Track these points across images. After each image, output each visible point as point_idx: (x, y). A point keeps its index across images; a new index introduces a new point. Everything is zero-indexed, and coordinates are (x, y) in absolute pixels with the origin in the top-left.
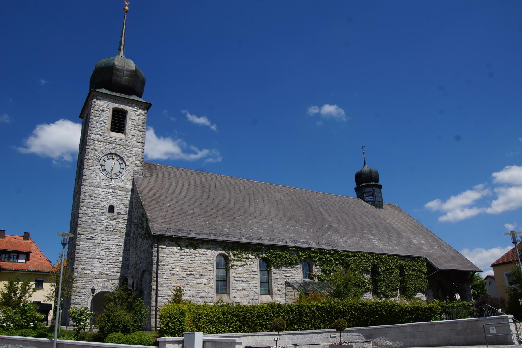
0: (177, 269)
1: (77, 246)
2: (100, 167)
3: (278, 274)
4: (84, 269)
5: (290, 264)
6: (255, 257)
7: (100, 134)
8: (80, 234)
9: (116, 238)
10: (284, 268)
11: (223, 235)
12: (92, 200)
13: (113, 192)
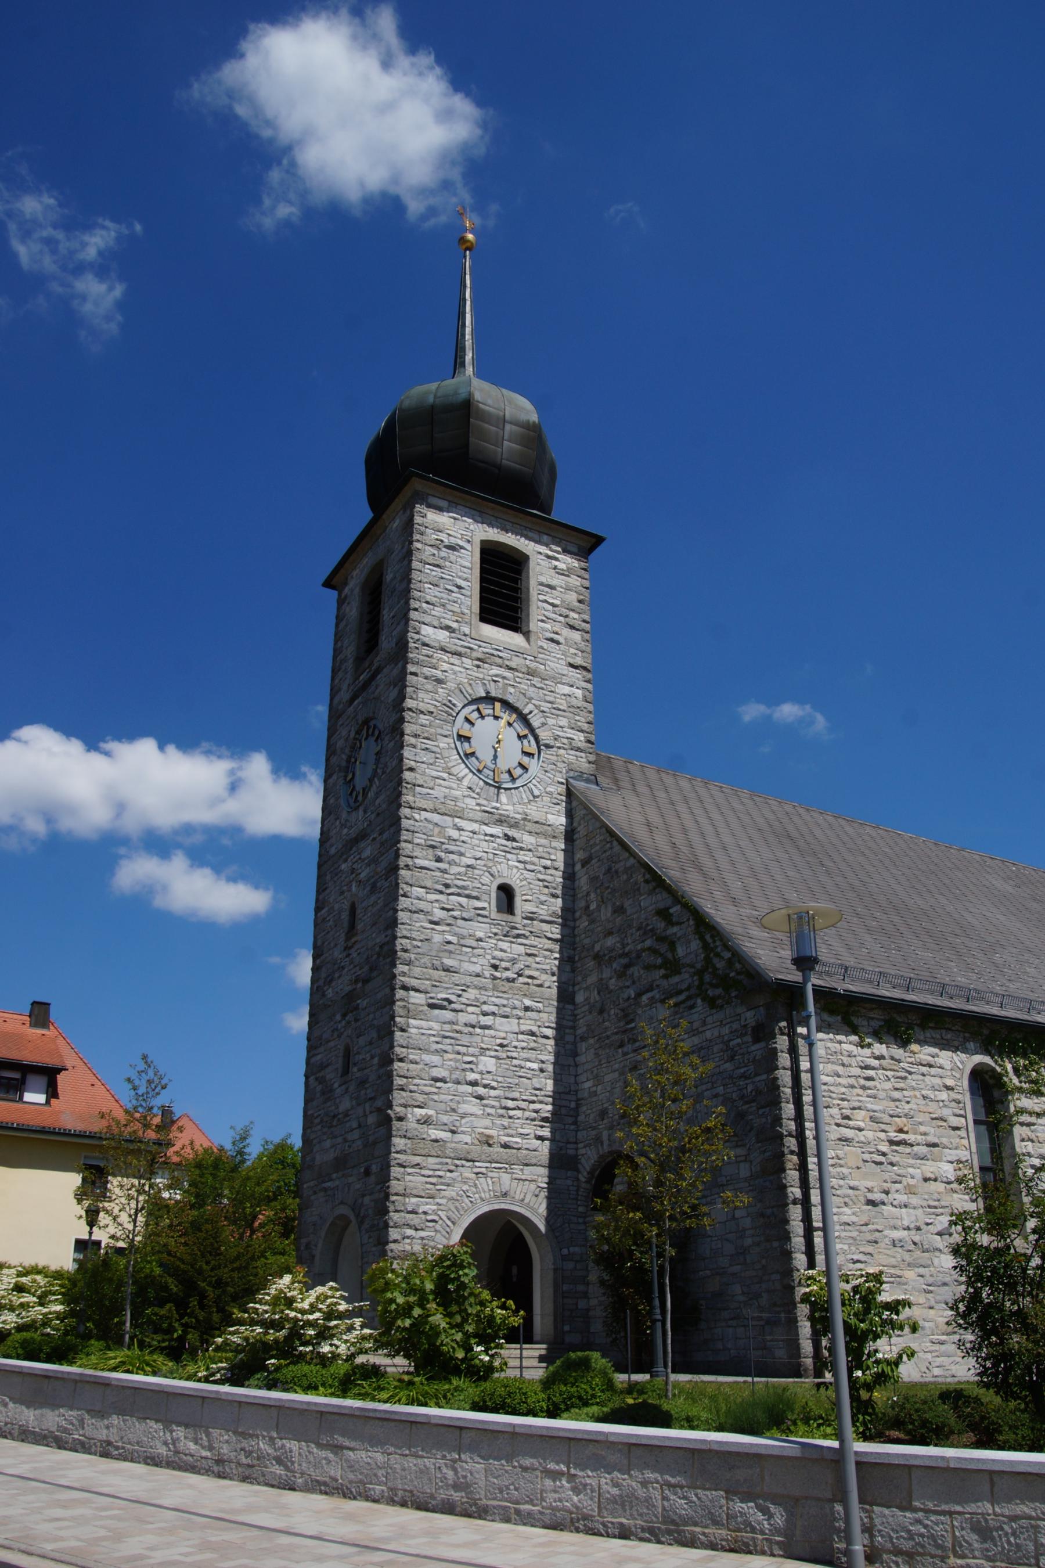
1: (398, 1034)
2: (458, 744)
7: (447, 628)
8: (405, 988)
9: (527, 1009)
12: (439, 860)
13: (508, 838)
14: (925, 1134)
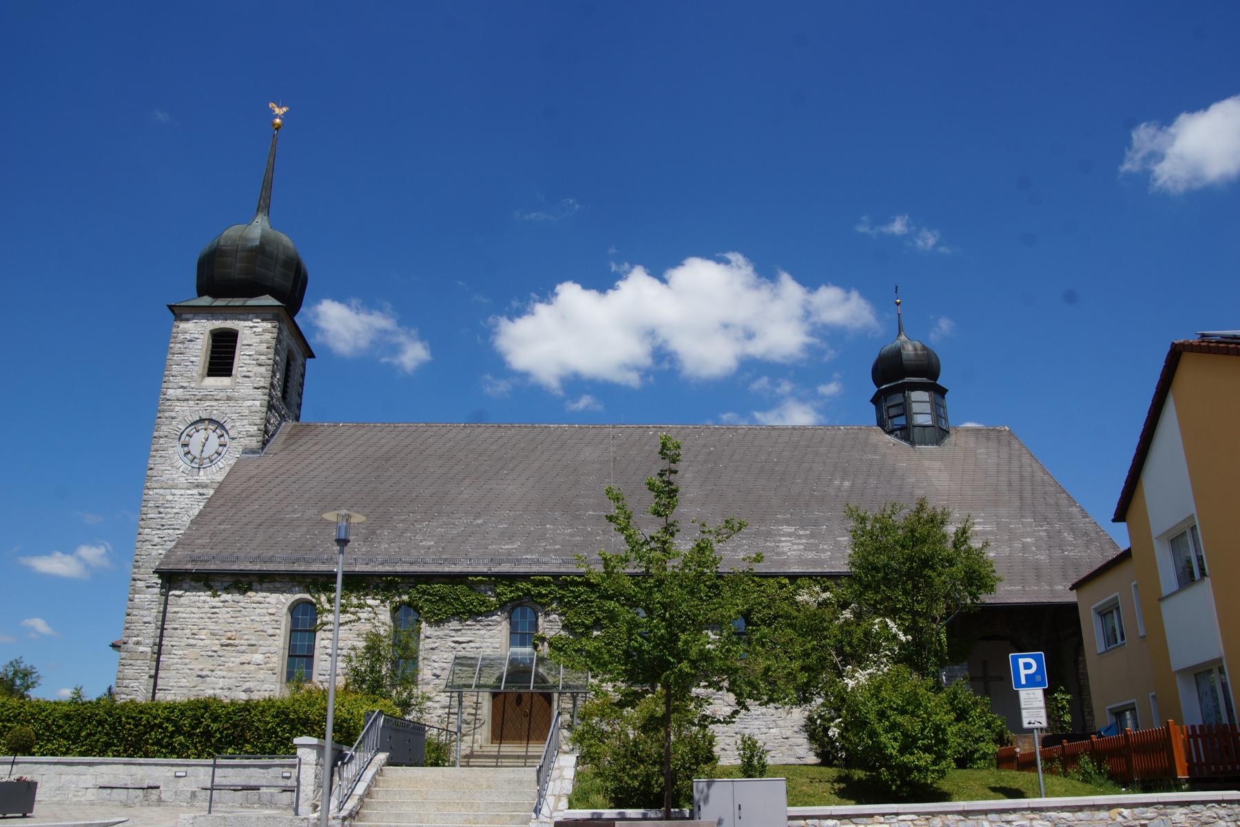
3: (438, 637)
4: (138, 643)
5: (472, 614)
7: (182, 387)
10: (454, 624)
11: (314, 561)
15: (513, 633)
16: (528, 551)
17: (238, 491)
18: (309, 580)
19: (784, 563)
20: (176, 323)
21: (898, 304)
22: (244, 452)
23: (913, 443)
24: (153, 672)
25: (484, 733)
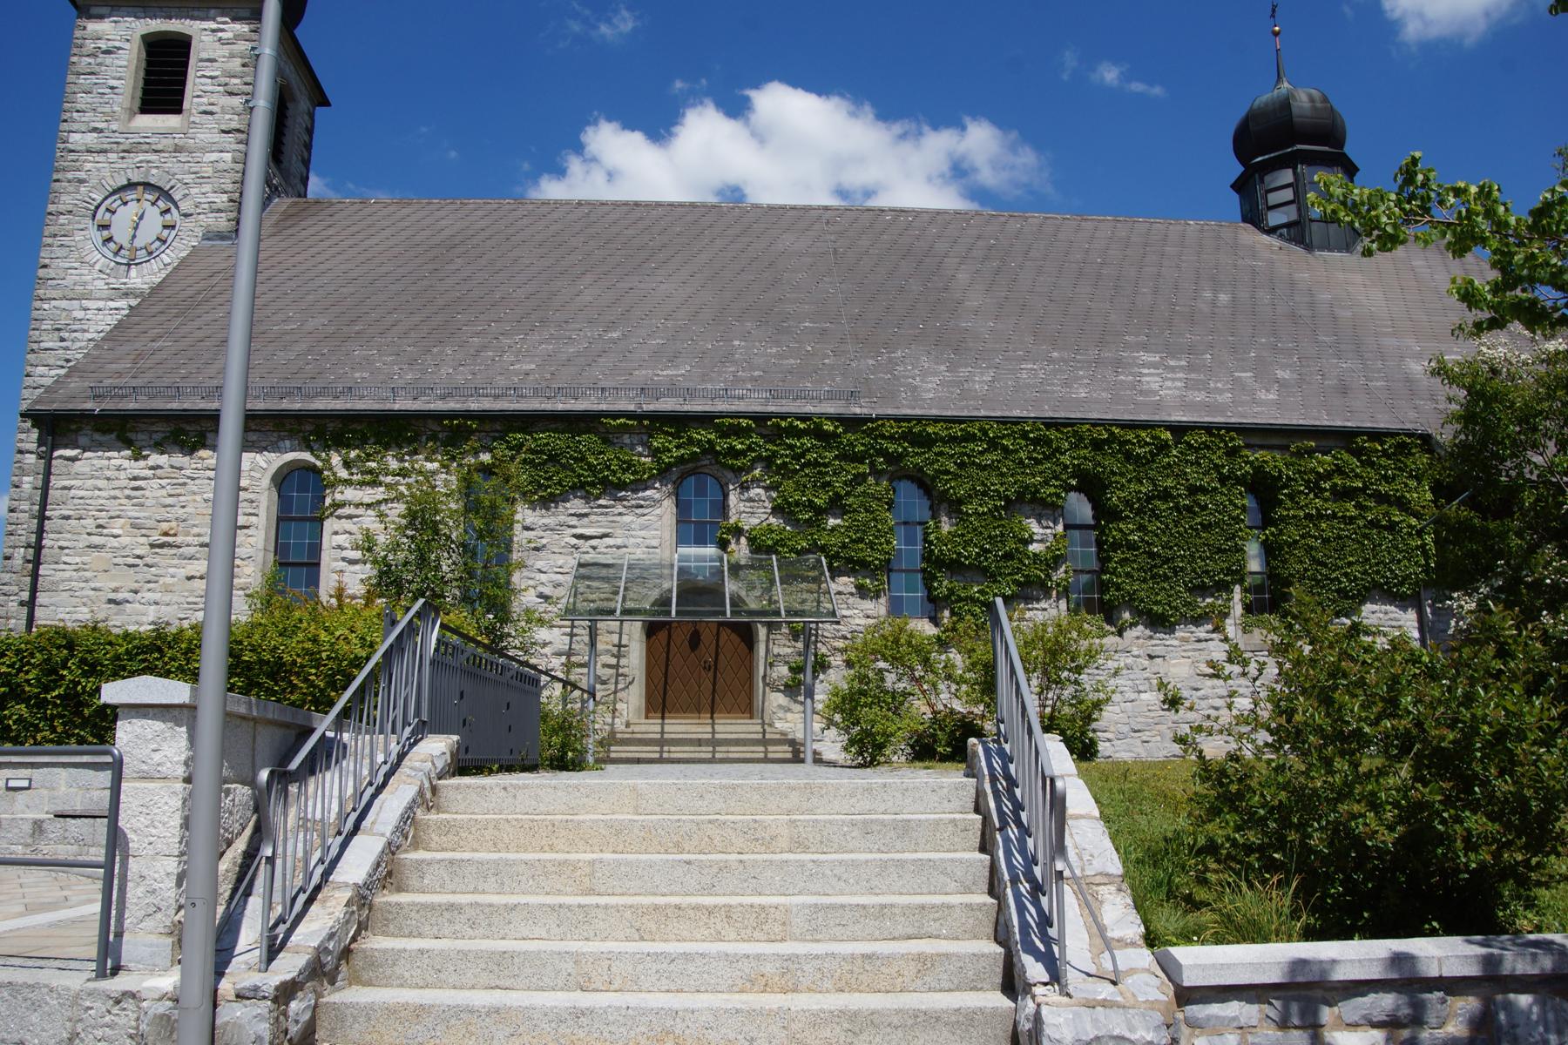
0: (117, 527)
3: (547, 528)
5: (607, 485)
6: (443, 466)
7: (95, 130)
10: (576, 505)
11: (318, 395)
12: (63, 340)
14: (199, 535)
15: (682, 518)
16: (704, 378)
17: (190, 292)
18: (309, 427)
19: (1158, 406)
20: (80, 22)
21: (1276, 34)
22: (206, 238)
23: (1309, 248)
24: (25, 596)
25: (632, 700)
